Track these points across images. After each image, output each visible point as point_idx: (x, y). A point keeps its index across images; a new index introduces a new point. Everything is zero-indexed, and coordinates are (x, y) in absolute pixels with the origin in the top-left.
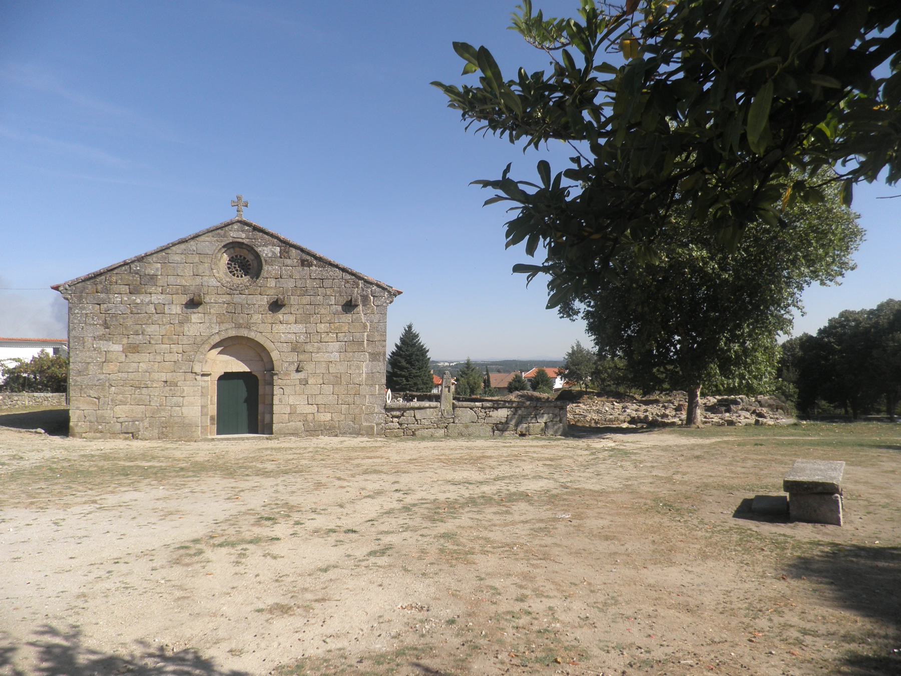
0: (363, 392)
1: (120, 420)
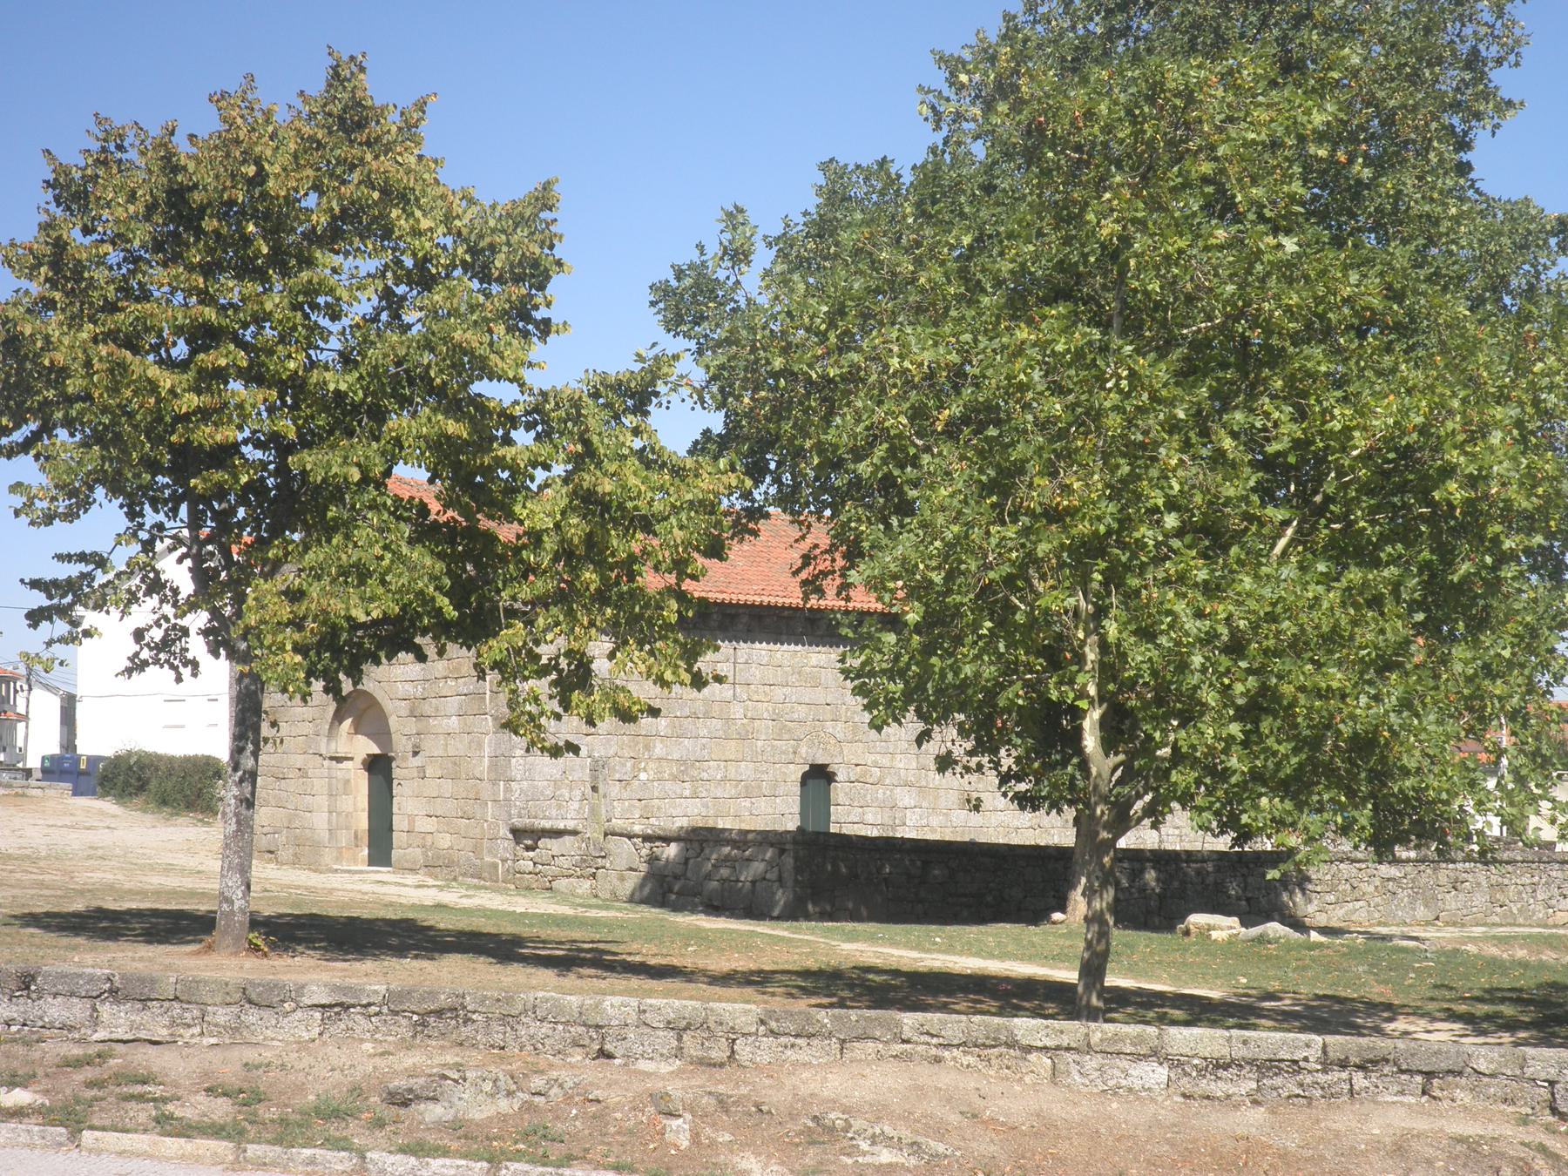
0: (485, 795)
1: (265, 830)
